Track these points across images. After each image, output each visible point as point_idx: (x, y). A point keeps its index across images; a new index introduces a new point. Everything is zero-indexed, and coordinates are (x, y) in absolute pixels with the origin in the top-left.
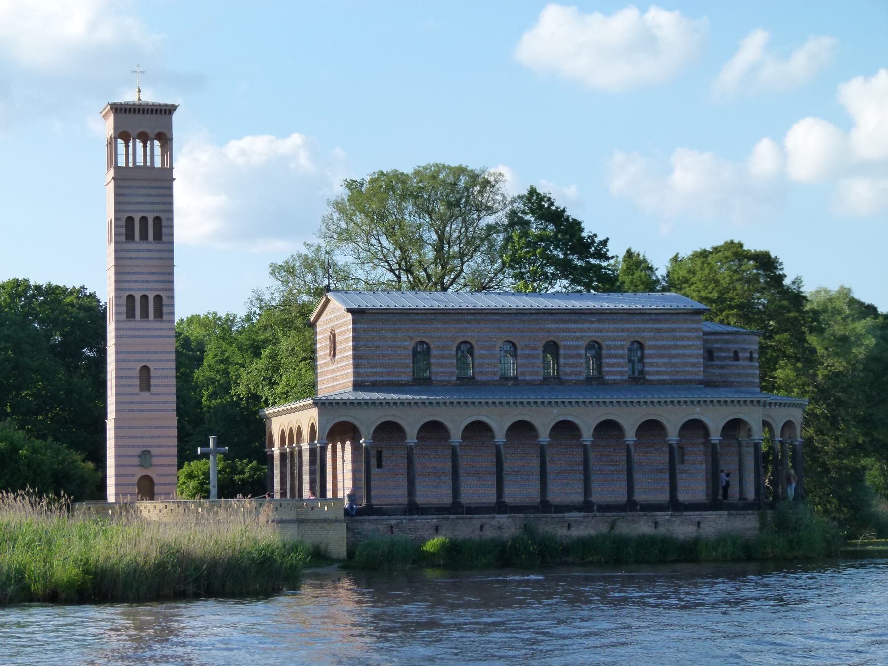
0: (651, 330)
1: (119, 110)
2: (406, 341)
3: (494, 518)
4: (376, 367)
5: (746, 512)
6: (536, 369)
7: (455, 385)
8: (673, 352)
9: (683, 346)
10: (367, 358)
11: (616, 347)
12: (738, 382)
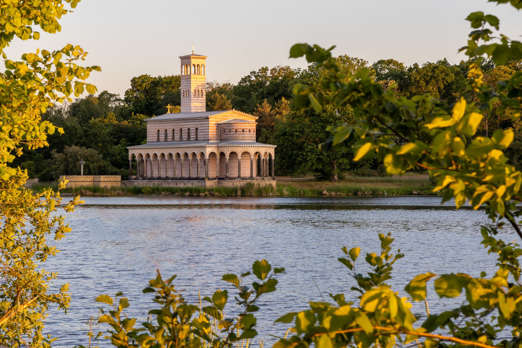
0: (199, 124)
1: (182, 58)
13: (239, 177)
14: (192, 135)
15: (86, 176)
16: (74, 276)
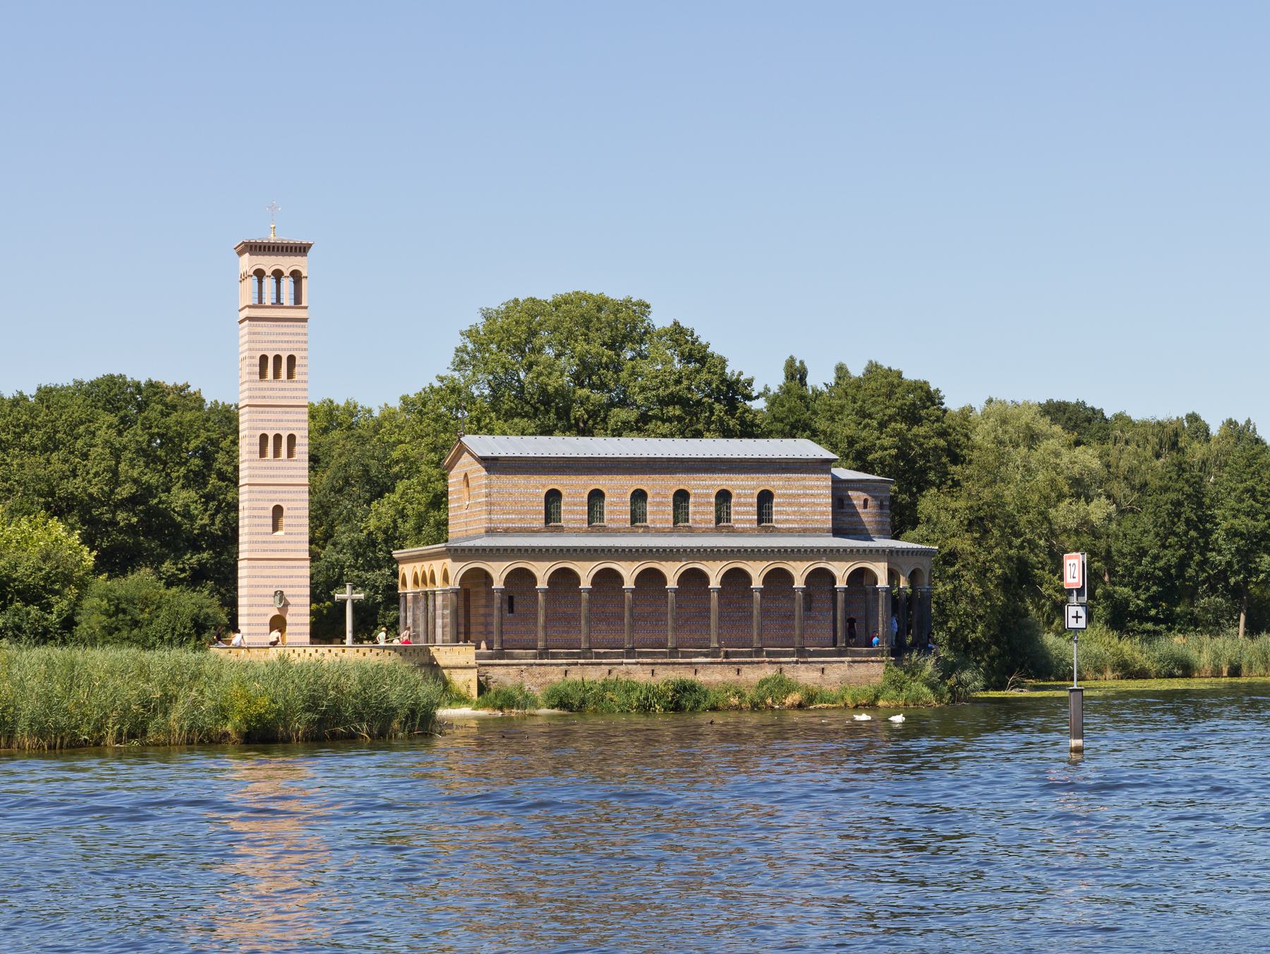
2: (538, 488)
3: (621, 664)
4: (509, 513)
5: (870, 659)
9: (812, 495)
10: (499, 505)
11: (746, 496)
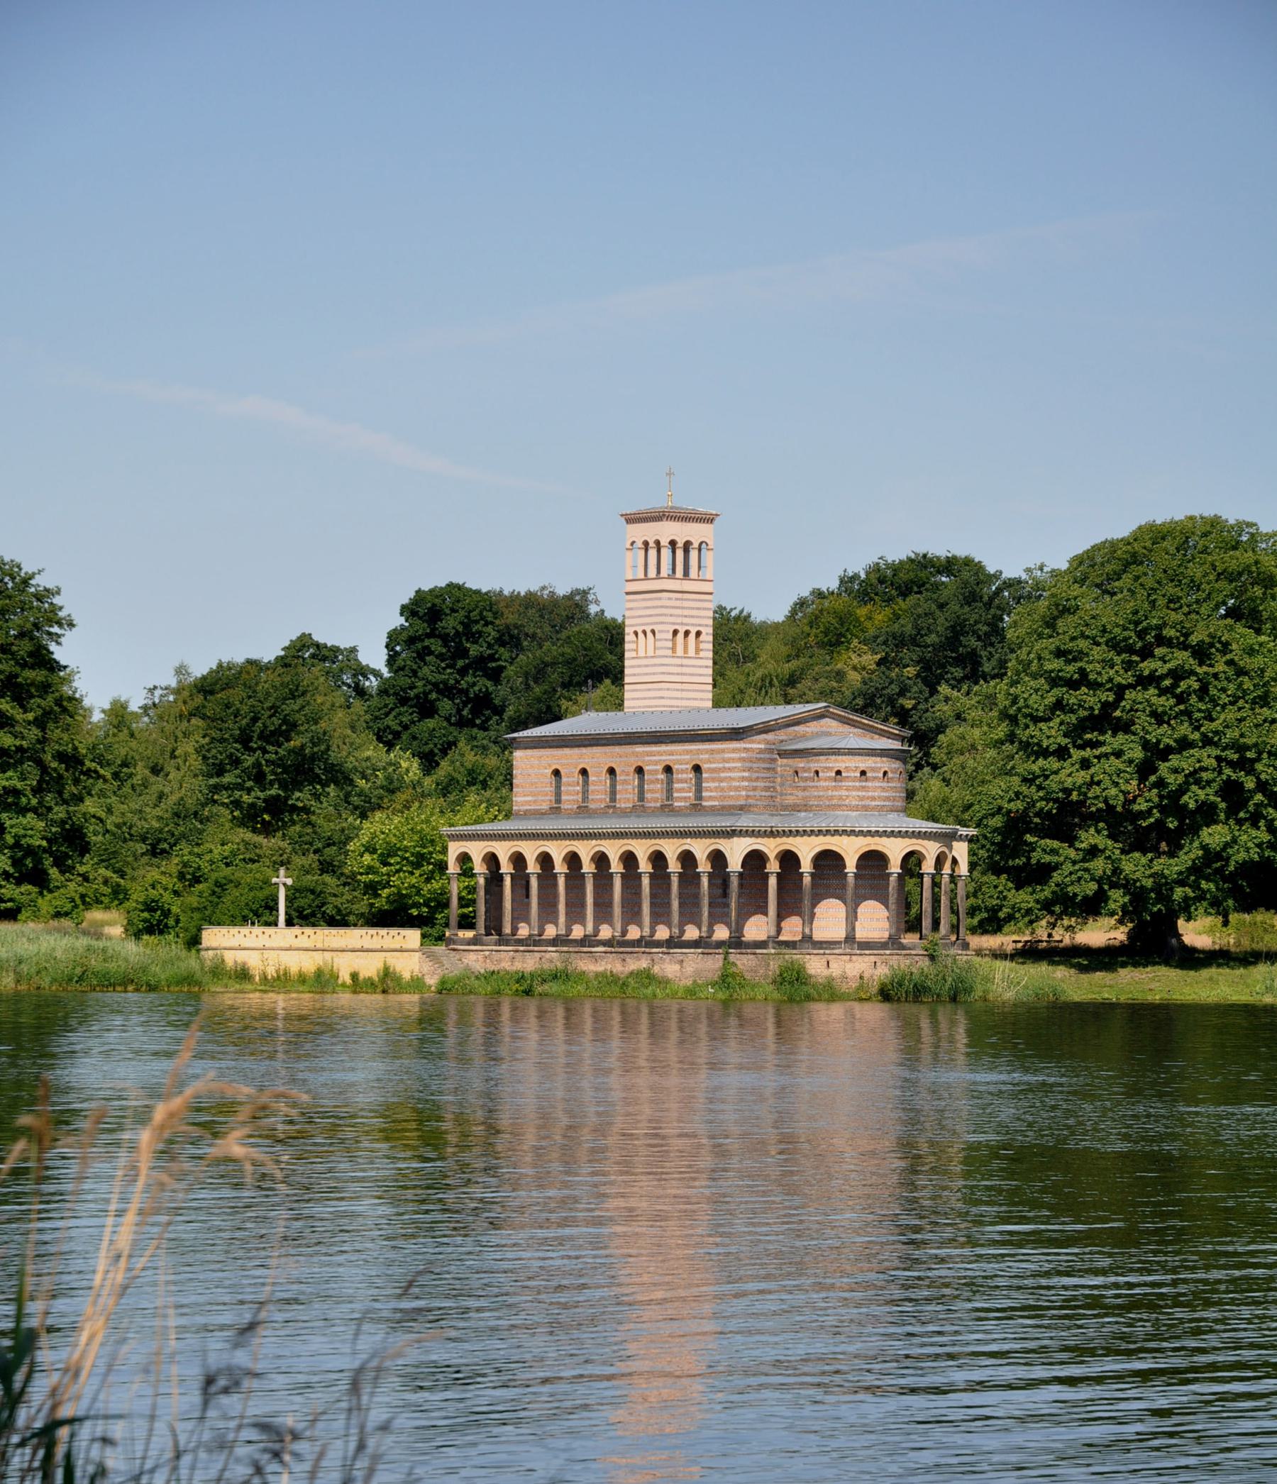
0: (707, 751)
6: (628, 796)
7: (576, 813)
8: (723, 775)
11: (682, 771)
12: (817, 806)
13: (850, 939)
14: (680, 790)
15: (296, 930)
16: (1123, 1444)
